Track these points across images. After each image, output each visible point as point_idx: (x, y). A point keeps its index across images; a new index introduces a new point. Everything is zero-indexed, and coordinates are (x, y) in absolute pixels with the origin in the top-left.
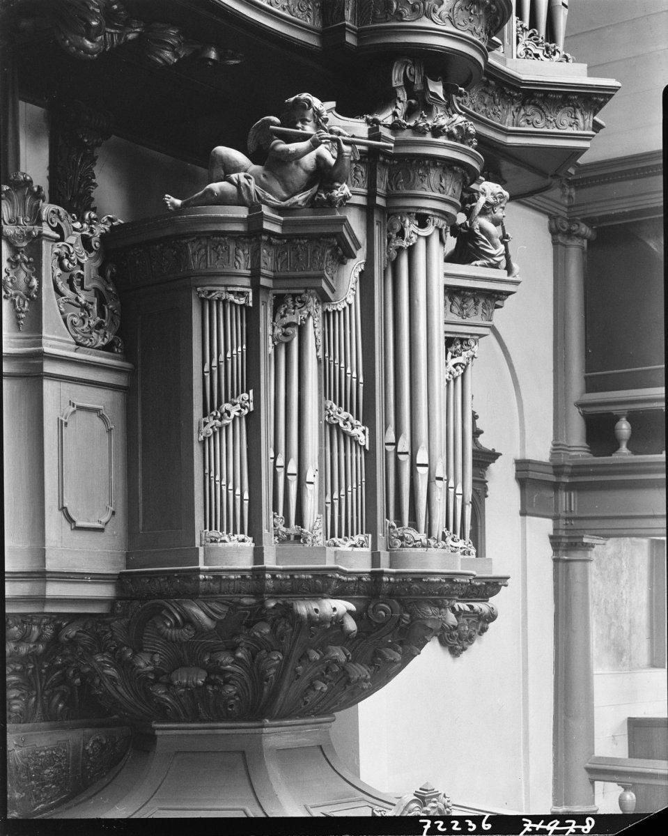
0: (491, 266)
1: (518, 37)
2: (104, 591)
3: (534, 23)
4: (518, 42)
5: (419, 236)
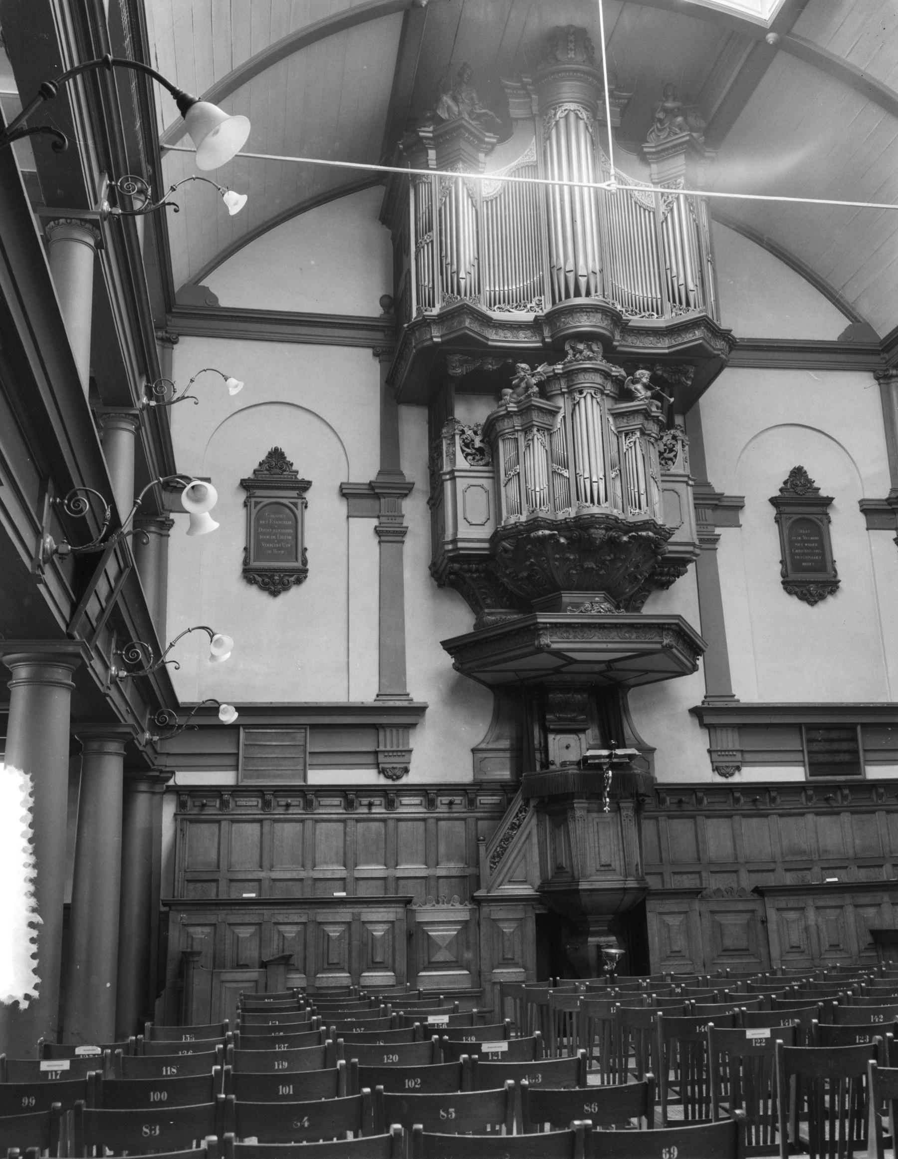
2: (486, 545)
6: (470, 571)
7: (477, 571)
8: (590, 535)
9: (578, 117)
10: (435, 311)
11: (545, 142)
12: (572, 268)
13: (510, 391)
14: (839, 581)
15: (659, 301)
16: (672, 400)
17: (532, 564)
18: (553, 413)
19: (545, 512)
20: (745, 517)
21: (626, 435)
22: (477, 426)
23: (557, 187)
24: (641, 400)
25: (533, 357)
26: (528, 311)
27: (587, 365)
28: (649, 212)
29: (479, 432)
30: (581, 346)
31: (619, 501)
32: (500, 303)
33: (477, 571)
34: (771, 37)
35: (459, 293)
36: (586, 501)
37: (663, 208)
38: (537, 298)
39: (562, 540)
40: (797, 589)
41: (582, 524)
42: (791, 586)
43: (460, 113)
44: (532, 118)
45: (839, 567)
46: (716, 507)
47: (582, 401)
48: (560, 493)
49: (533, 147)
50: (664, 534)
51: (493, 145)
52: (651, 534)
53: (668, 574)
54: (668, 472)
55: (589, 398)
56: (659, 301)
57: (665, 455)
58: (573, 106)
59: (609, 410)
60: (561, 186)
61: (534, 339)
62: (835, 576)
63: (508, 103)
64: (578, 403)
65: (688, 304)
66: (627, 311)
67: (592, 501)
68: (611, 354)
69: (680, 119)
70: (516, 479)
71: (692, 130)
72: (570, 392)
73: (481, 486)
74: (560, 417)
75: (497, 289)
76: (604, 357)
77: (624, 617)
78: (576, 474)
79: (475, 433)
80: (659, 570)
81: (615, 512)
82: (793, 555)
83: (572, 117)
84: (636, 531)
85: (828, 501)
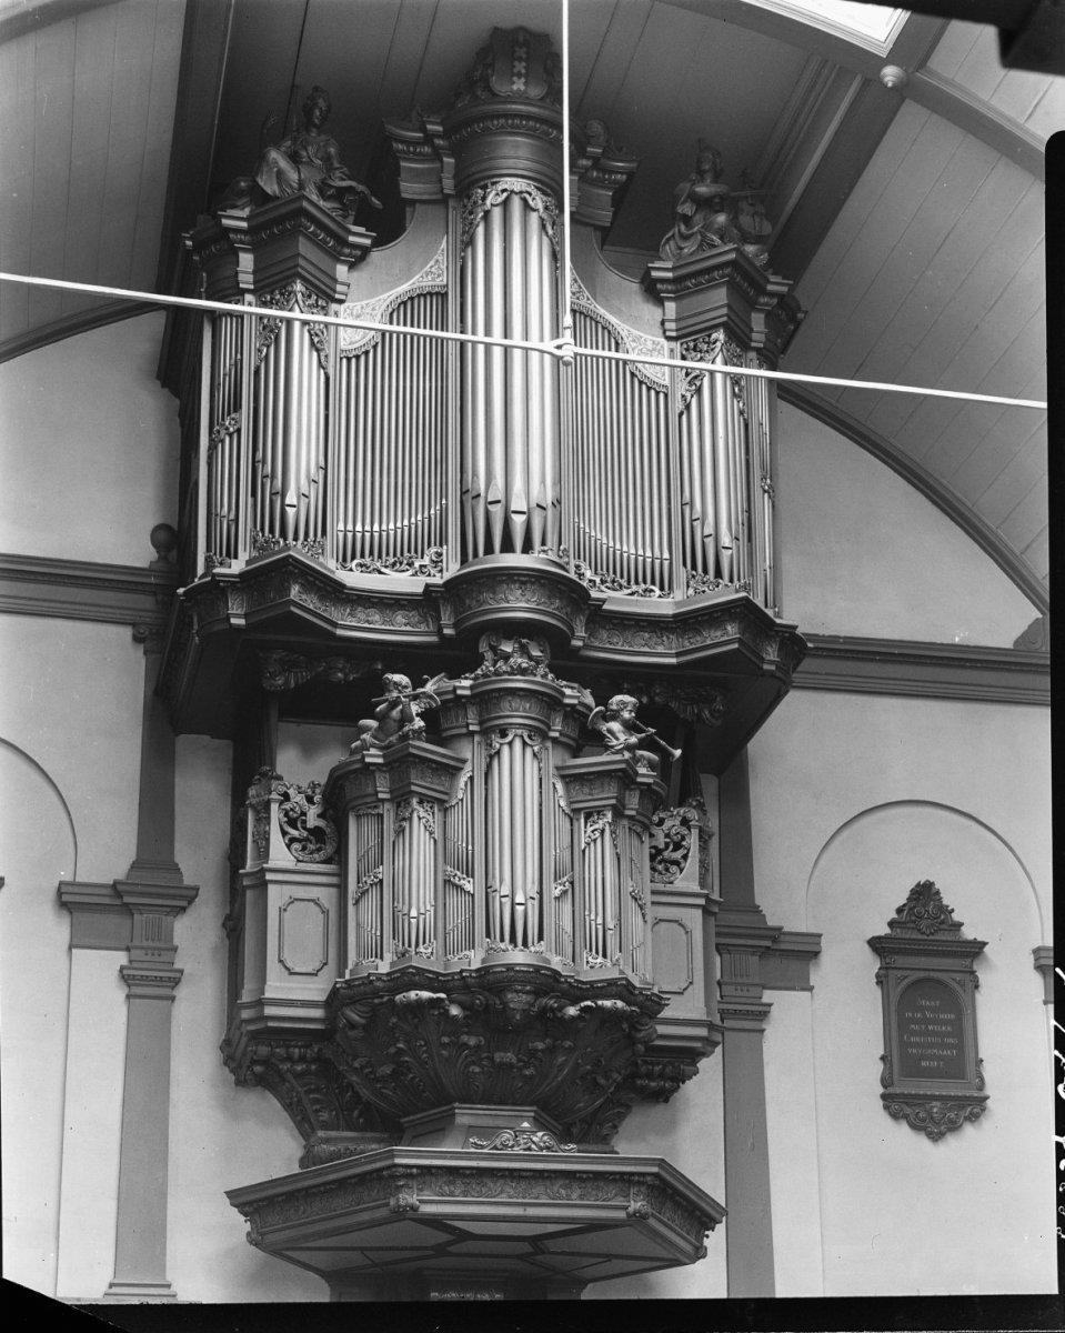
0: (613, 753)
1: (688, 583)
2: (318, 1013)
3: (705, 571)
4: (688, 586)
5: (501, 744)
6: (289, 1058)
7: (302, 1059)
8: (505, 1004)
9: (527, 207)
10: (237, 566)
11: (464, 250)
12: (500, 496)
13: (373, 723)
14: (987, 1098)
15: (666, 563)
16: (678, 753)
17: (400, 1052)
18: (452, 771)
19: (428, 957)
20: (824, 973)
21: (588, 816)
22: (314, 786)
23: (481, 348)
24: (618, 752)
25: (417, 662)
26: (415, 574)
27: (519, 683)
28: (657, 393)
29: (317, 798)
30: (507, 647)
31: (567, 940)
32: (362, 556)
33: (302, 1059)
34: (890, 74)
35: (284, 534)
36: (502, 940)
37: (682, 387)
38: (434, 550)
39: (455, 1011)
40: (908, 1110)
41: (491, 982)
42: (898, 1104)
43: (301, 186)
44: (444, 201)
45: (989, 1072)
46: (766, 952)
47: (506, 749)
48: (456, 919)
49: (441, 257)
50: (649, 1005)
51: (365, 251)
52: (620, 1004)
53: (661, 1076)
54: (669, 888)
55: (518, 745)
56: (666, 563)
57: (666, 854)
58: (518, 184)
59: (558, 768)
60: (488, 347)
61: (423, 628)
62: (981, 1086)
63: (398, 168)
64: (498, 753)
65: (718, 574)
66: (603, 582)
67: (513, 940)
68: (567, 663)
69: (721, 218)
70: (375, 892)
71: (746, 238)
72: (485, 732)
73: (315, 902)
74: (463, 779)
75: (359, 528)
76: (552, 668)
77: (571, 1157)
78: (487, 888)
79: (310, 800)
80: (643, 1069)
81: (556, 962)
82: (903, 1045)
83: (516, 204)
84: (594, 998)
85: (976, 949)
